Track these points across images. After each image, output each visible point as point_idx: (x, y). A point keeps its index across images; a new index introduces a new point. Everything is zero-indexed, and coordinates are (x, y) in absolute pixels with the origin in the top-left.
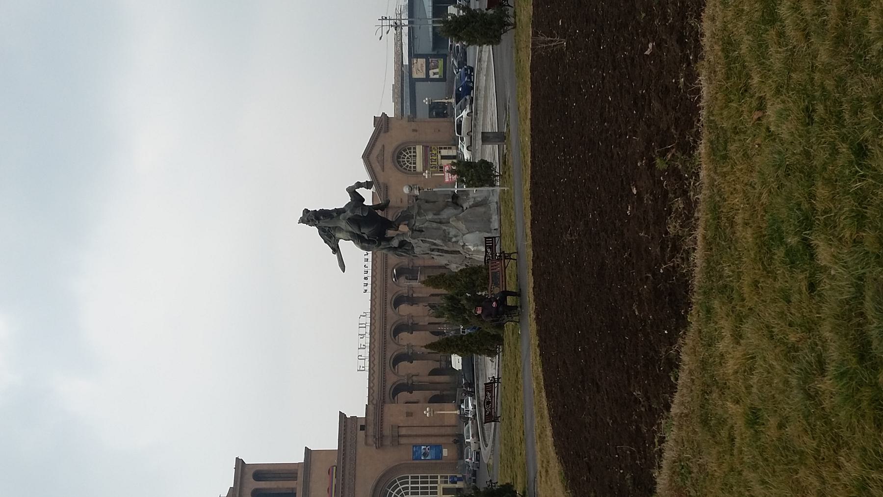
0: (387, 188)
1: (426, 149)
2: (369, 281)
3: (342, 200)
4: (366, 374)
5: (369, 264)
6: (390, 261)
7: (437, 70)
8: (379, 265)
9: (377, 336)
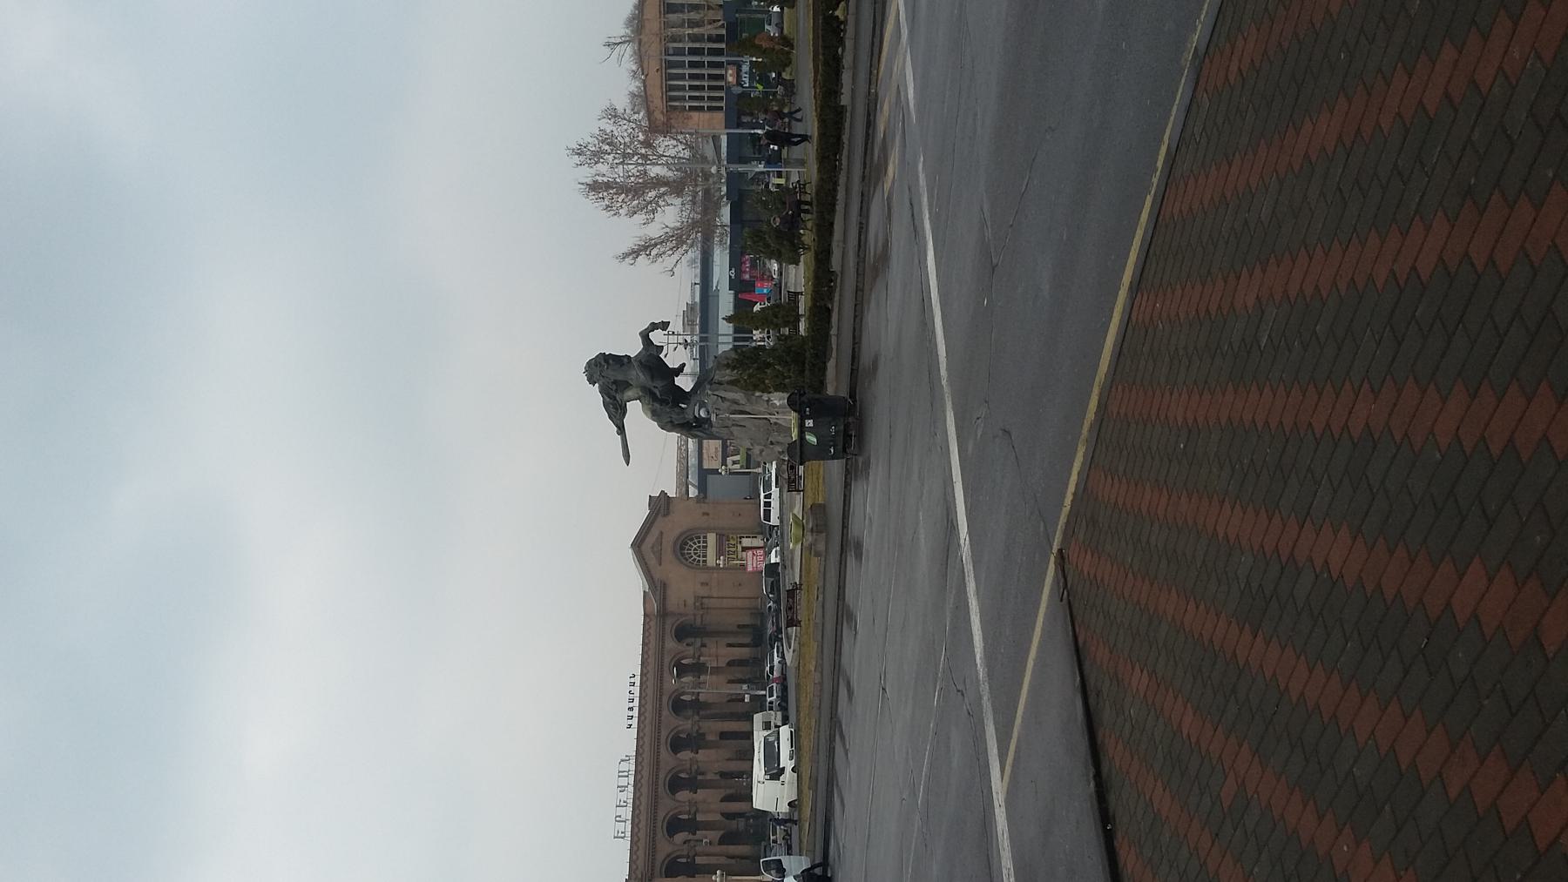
0: (664, 586)
1: (722, 538)
2: (635, 713)
3: (634, 348)
4: (626, 844)
5: (637, 690)
6: (666, 686)
7: (737, 458)
8: (650, 691)
9: (644, 790)
